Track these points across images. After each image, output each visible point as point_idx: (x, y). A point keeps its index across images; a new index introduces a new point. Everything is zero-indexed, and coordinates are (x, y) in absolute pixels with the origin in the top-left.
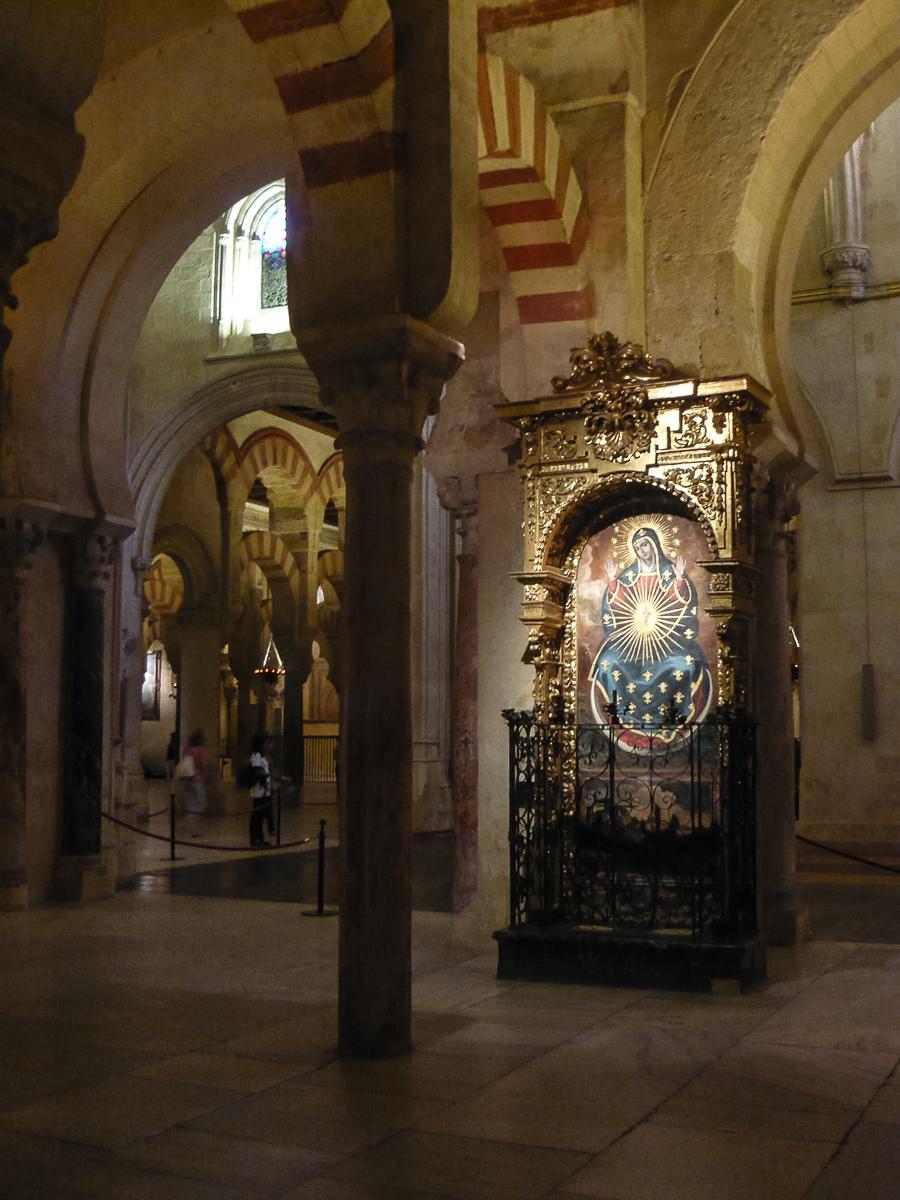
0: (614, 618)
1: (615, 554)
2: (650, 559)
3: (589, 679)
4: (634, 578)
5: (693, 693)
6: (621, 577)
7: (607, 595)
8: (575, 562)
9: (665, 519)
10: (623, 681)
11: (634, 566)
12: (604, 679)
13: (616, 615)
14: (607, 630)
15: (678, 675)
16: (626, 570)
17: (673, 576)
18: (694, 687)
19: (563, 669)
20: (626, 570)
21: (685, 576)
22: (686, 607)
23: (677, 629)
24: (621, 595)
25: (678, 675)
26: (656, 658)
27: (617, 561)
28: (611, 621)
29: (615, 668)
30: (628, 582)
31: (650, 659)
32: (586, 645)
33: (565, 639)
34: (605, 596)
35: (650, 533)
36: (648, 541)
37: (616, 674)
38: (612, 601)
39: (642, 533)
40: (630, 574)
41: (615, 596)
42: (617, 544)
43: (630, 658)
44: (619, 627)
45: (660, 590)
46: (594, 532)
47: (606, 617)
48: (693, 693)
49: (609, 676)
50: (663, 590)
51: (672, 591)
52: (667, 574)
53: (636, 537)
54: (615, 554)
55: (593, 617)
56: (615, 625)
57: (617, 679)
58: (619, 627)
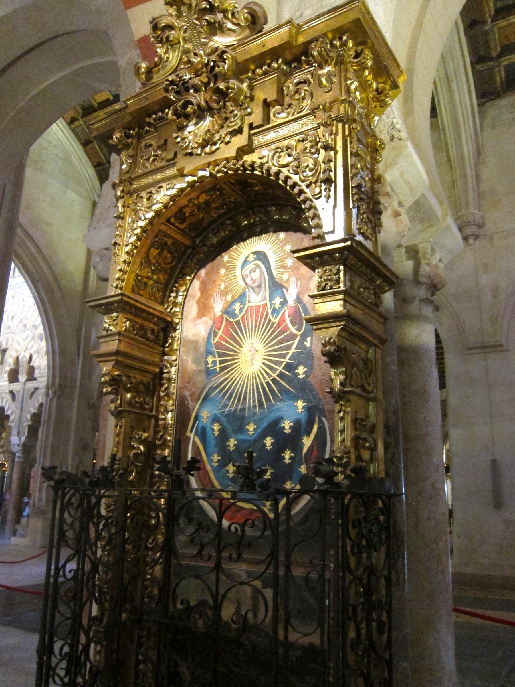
0: (218, 359)
1: (223, 286)
2: (259, 286)
3: (188, 434)
4: (241, 310)
5: (305, 450)
6: (228, 311)
7: (212, 333)
8: (180, 299)
9: (277, 238)
10: (224, 436)
11: (242, 298)
12: (203, 434)
13: (220, 355)
14: (209, 373)
15: (287, 425)
16: (234, 302)
17: (284, 302)
18: (307, 442)
19: (157, 425)
20: (234, 302)
21: (299, 300)
22: (298, 339)
23: (289, 367)
24: (226, 332)
25: (287, 425)
26: (261, 405)
27: (224, 293)
28: (214, 362)
29: (215, 419)
30: (234, 315)
31: (254, 406)
32: (187, 393)
33: (162, 385)
34: (210, 334)
35: (261, 256)
36: (258, 266)
37: (216, 427)
38: (217, 339)
39: (252, 257)
40: (237, 307)
41: (220, 333)
42: (225, 275)
43: (232, 407)
44: (222, 369)
45: (270, 321)
46: (202, 264)
47: (210, 359)
48: (305, 450)
49: (209, 431)
50: (273, 320)
51: (282, 320)
52: (277, 301)
53: (245, 262)
54: (223, 286)
55: (196, 361)
56: (218, 366)
57: (216, 433)
58: (222, 369)
